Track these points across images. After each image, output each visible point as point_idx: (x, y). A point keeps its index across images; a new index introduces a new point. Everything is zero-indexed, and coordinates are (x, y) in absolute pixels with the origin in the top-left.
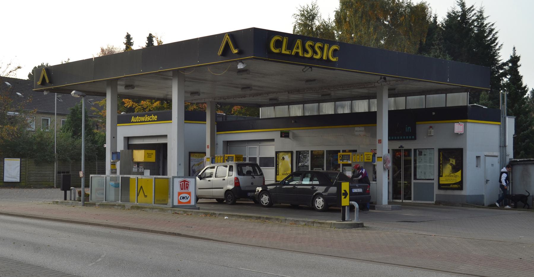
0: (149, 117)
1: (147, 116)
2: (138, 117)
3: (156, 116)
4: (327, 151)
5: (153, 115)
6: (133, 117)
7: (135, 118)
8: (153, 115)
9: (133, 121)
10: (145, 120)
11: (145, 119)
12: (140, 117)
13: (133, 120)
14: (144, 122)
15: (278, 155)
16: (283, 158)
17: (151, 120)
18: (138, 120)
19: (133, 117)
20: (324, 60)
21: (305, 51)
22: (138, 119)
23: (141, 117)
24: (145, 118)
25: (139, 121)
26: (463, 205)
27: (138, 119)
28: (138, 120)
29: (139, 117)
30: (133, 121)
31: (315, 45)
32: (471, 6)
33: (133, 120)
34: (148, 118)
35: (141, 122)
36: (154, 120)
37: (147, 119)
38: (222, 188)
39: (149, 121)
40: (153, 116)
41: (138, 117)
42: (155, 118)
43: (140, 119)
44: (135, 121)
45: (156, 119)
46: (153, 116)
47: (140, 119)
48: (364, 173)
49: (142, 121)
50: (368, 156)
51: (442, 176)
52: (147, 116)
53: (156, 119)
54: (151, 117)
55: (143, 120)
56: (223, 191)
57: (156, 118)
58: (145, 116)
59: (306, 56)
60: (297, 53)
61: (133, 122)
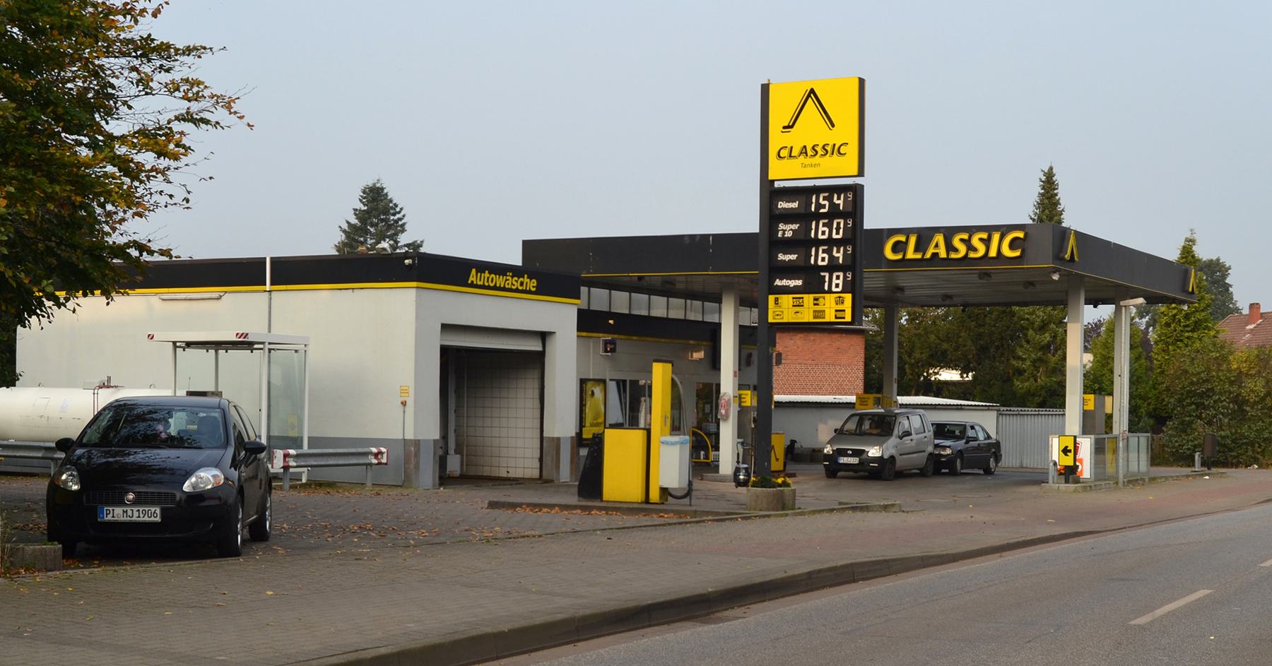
1: (512, 277)
2: (487, 274)
3: (534, 280)
4: (630, 381)
5: (526, 276)
6: (474, 271)
7: (479, 274)
8: (526, 276)
9: (472, 282)
10: (507, 286)
11: (507, 282)
12: (493, 275)
13: (474, 280)
14: (504, 289)
15: (584, 385)
16: (593, 393)
17: (520, 288)
18: (488, 282)
19: (474, 271)
22: (488, 278)
23: (496, 275)
24: (506, 280)
25: (492, 285)
27: (488, 278)
28: (488, 282)
29: (490, 273)
30: (472, 282)
33: (474, 280)
34: (515, 283)
35: (495, 288)
36: (528, 289)
37: (512, 284)
39: (517, 291)
40: (526, 280)
41: (487, 272)
42: (532, 284)
43: (492, 279)
44: (479, 283)
45: (533, 287)
47: (492, 279)
49: (498, 285)
51: (584, 427)
52: (512, 277)
53: (533, 287)
54: (521, 279)
55: (502, 286)
56: (926, 454)
57: (535, 285)
61: (473, 285)
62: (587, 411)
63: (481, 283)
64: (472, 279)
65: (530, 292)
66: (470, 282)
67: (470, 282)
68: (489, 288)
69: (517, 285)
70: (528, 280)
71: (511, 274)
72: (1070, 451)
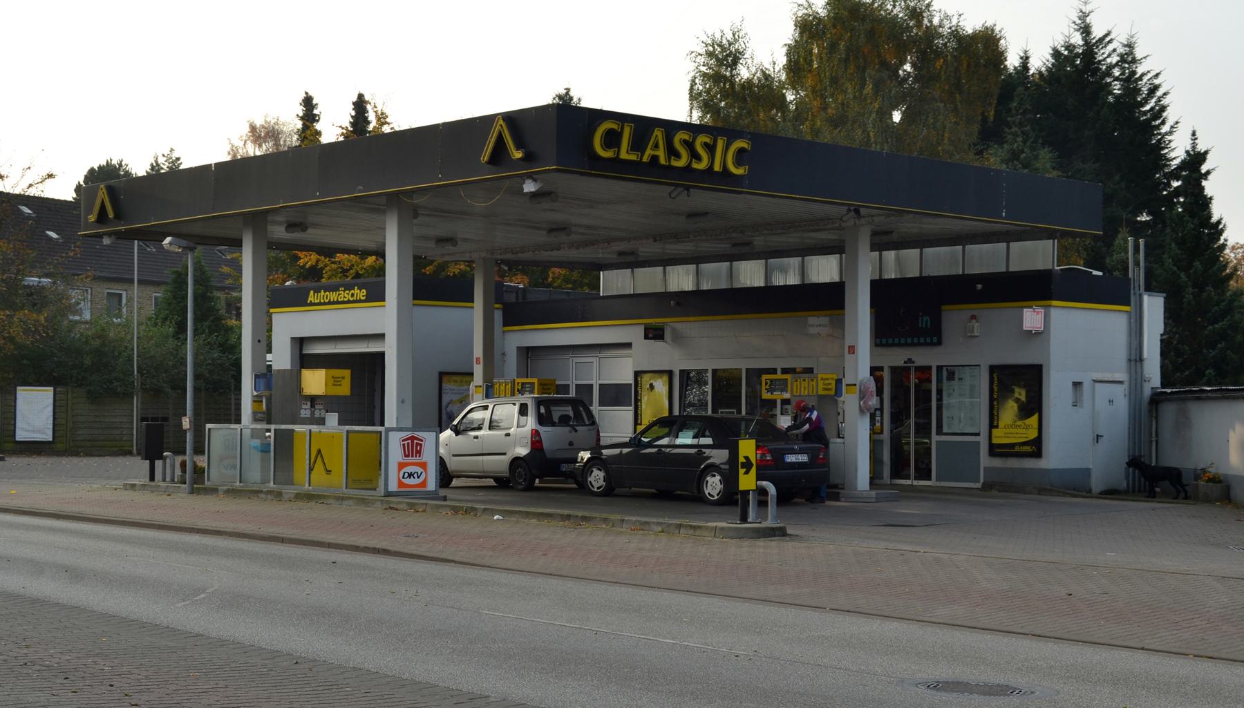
0: (347, 292)
1: (344, 291)
3: (364, 290)
4: (747, 370)
5: (356, 288)
6: (312, 292)
8: (356, 288)
9: (311, 301)
10: (340, 300)
12: (327, 293)
14: (338, 303)
15: (639, 379)
16: (652, 387)
17: (351, 299)
19: (312, 292)
20: (717, 172)
21: (672, 152)
23: (329, 292)
24: (339, 295)
25: (327, 301)
26: (1042, 491)
29: (325, 292)
30: (311, 301)
31: (694, 139)
32: (1106, 32)
34: (346, 295)
35: (330, 303)
38: (505, 454)
39: (349, 302)
40: (356, 291)
42: (362, 294)
43: (327, 296)
45: (363, 296)
46: (358, 289)
47: (327, 296)
48: (814, 419)
49: (332, 300)
50: (827, 382)
51: (997, 427)
52: (344, 291)
53: (363, 296)
54: (352, 291)
55: (335, 300)
56: (506, 459)
57: (365, 294)
58: (339, 291)
59: (675, 163)
60: (655, 158)
61: (312, 304)
62: (643, 407)
63: (318, 301)
64: (311, 298)
65: (360, 301)
66: (309, 302)
67: (309, 302)
68: (325, 304)
69: (349, 297)
70: (359, 291)
71: (343, 289)
72: (743, 465)
